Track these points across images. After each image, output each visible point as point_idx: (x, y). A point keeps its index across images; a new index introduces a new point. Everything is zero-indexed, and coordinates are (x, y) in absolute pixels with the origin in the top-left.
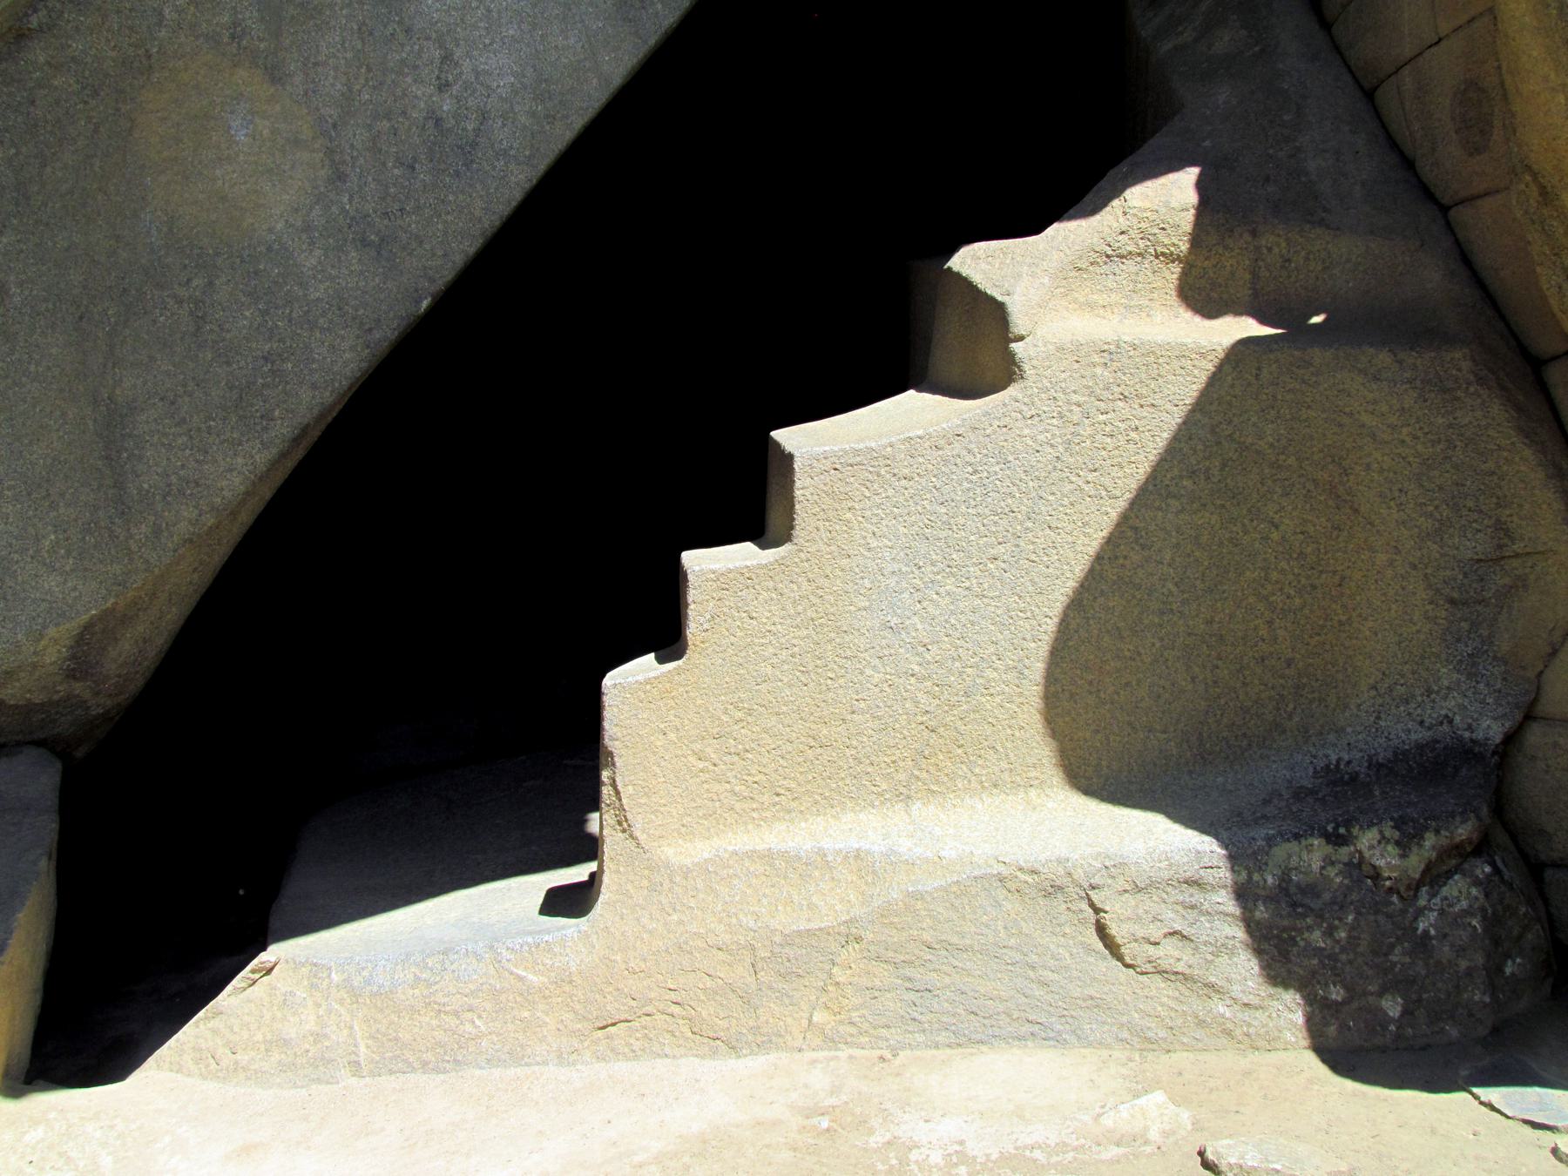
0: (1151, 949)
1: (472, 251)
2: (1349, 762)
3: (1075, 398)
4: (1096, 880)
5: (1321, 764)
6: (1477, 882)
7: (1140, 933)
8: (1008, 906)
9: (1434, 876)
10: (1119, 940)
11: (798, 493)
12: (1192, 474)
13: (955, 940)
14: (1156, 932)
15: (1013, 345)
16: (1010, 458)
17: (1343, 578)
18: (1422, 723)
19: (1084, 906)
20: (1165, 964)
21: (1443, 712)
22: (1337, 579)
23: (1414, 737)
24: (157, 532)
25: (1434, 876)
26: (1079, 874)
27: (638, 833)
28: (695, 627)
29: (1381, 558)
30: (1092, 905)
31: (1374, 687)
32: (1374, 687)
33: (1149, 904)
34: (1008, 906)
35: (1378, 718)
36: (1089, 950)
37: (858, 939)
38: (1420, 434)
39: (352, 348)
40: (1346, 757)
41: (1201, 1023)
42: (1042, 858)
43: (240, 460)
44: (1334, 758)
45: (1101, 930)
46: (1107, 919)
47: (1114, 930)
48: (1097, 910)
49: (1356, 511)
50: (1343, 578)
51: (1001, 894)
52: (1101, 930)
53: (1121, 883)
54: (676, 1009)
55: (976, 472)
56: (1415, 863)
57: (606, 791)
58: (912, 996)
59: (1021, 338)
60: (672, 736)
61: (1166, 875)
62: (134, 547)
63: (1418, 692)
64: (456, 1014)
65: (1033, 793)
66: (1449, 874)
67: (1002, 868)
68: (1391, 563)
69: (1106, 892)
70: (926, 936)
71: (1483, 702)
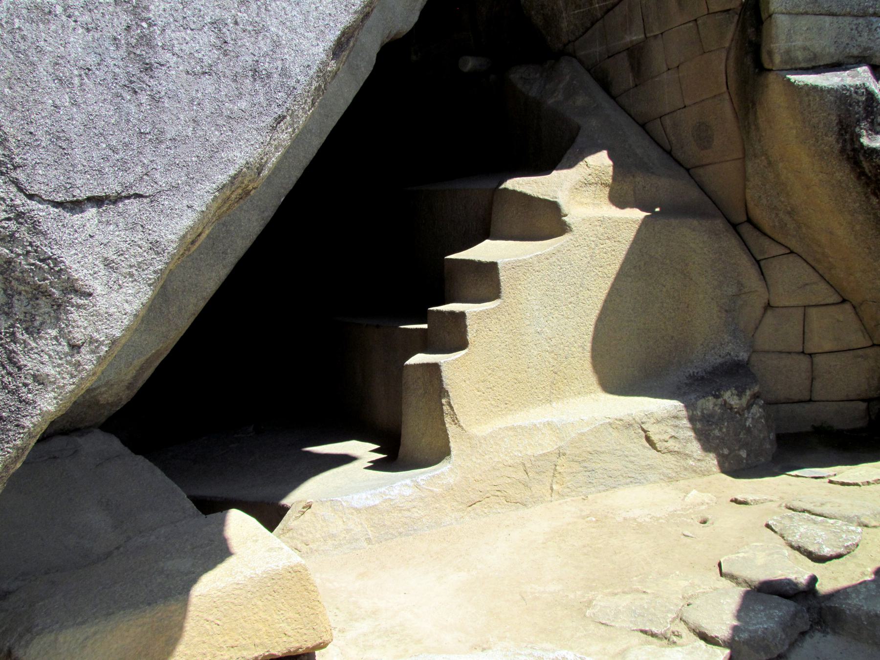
0: (666, 444)
1: (299, 175)
3: (592, 239)
4: (644, 420)
5: (687, 375)
6: (760, 407)
8: (614, 434)
11: (501, 278)
13: (599, 449)
14: (666, 437)
19: (640, 431)
20: (671, 448)
24: (180, 310)
25: (749, 406)
26: (637, 419)
27: (462, 424)
28: (471, 336)
29: (701, 296)
30: (643, 430)
33: (662, 427)
34: (614, 434)
36: (644, 447)
37: (564, 454)
39: (257, 220)
41: (686, 469)
42: (622, 414)
43: (214, 274)
44: (691, 372)
45: (648, 439)
46: (650, 434)
47: (654, 438)
48: (645, 431)
51: (611, 430)
52: (648, 439)
53: (652, 420)
54: (498, 493)
56: (744, 401)
57: (446, 408)
58: (588, 473)
60: (468, 382)
61: (666, 415)
62: (171, 318)
64: (409, 510)
65: (593, 395)
66: (752, 405)
67: (608, 420)
68: (704, 298)
70: (589, 449)
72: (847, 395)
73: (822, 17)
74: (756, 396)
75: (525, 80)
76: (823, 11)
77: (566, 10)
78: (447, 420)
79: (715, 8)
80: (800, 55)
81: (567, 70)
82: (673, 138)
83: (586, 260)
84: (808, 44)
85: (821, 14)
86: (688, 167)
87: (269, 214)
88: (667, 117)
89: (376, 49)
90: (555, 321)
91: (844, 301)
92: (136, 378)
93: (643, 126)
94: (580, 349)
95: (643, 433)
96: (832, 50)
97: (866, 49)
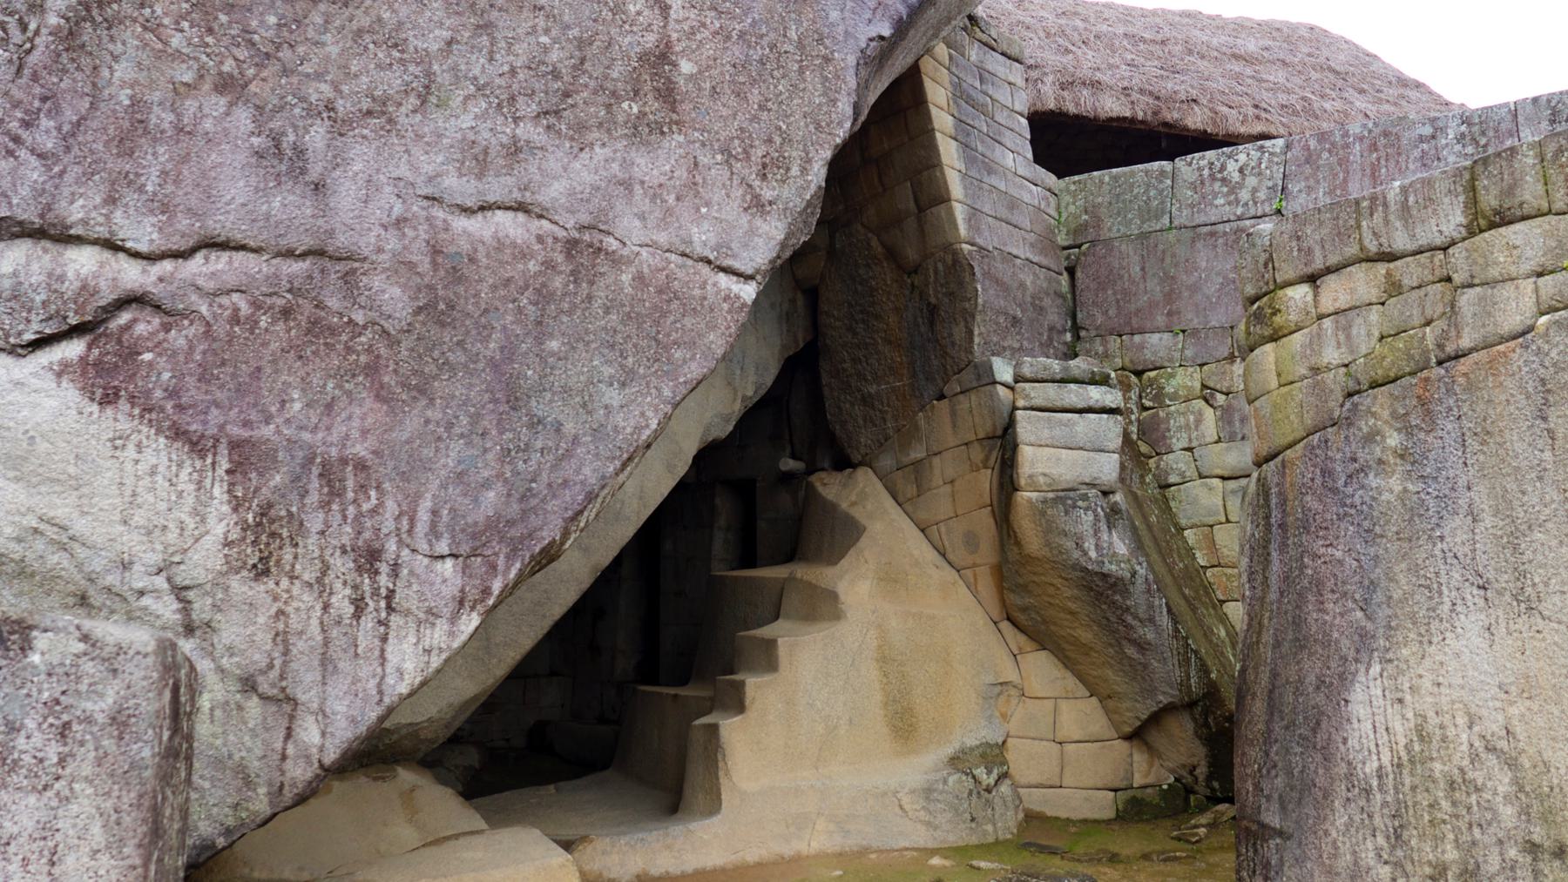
45: (901, 807)
52: (901, 807)
57: (721, 764)
75: (830, 486)
78: (721, 774)
79: (981, 435)
80: (1041, 479)
81: (865, 479)
87: (586, 585)
89: (694, 451)
92: (454, 718)
93: (923, 531)
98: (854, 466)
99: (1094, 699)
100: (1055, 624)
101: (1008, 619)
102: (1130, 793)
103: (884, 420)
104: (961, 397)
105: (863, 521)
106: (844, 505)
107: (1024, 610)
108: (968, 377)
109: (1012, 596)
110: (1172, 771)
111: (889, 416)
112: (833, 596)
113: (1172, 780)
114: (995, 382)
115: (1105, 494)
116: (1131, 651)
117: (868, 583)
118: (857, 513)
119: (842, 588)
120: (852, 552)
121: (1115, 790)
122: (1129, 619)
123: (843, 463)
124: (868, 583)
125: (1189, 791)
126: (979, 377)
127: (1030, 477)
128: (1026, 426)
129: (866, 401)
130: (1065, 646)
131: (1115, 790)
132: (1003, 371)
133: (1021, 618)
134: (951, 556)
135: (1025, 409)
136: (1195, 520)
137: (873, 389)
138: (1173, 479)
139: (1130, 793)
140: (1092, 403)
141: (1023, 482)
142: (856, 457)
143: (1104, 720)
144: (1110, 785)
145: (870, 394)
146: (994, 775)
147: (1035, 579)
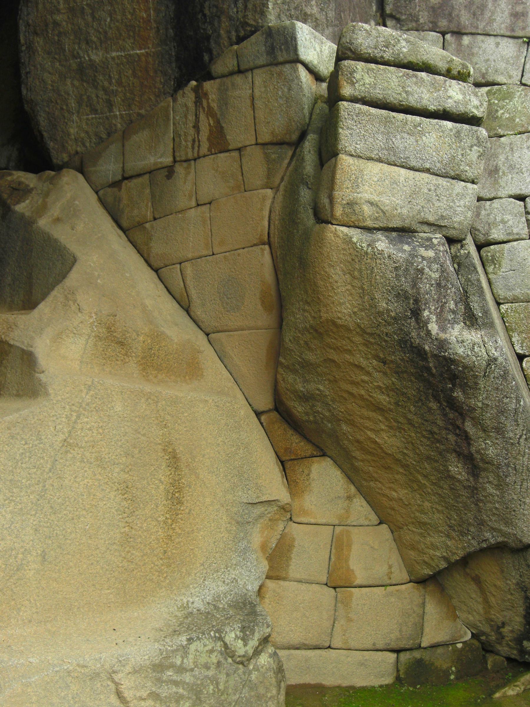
2: (193, 603)
4: (116, 668)
7: (138, 695)
9: (257, 652)
10: (128, 699)
12: (127, 455)
15: (37, 375)
16: (43, 437)
17: (190, 510)
18: (224, 582)
21: (233, 576)
22: (187, 511)
23: (221, 589)
30: (113, 681)
31: (202, 565)
32: (202, 565)
35: (205, 580)
38: (226, 441)
40: (191, 600)
44: (185, 600)
45: (119, 695)
47: (128, 694)
48: (117, 684)
49: (198, 477)
50: (190, 510)
52: (119, 695)
53: (128, 669)
55: (26, 443)
59: (43, 372)
63: (222, 567)
65: (49, 625)
69: (120, 675)
71: (250, 571)
72: (374, 644)
73: (396, 168)
74: (265, 640)
76: (398, 162)
77: (78, 112)
79: (266, 138)
80: (367, 209)
82: (193, 293)
83: (62, 437)
84: (375, 198)
85: (395, 165)
86: (207, 330)
88: (188, 264)
90: (9, 516)
91: (380, 523)
94: (40, 558)
95: (112, 686)
96: (405, 211)
97: (442, 217)
98: (58, 168)
99: (384, 526)
100: (351, 423)
101: (276, 409)
102: (417, 654)
103: (110, 105)
104: (238, 79)
105: (73, 247)
106: (43, 223)
107: (305, 398)
108: (254, 48)
109: (291, 378)
110: (469, 626)
111: (118, 100)
112: (28, 359)
113: (469, 635)
114: (297, 60)
115: (451, 241)
116: (457, 469)
117: (82, 341)
118: (62, 234)
119: (41, 348)
120: (56, 293)
121: (398, 651)
122: (469, 427)
123: (38, 159)
124: (82, 341)
125: (487, 649)
126: (271, 51)
127: (351, 204)
128: (356, 129)
129: (85, 72)
130: (357, 454)
131: (398, 651)
132: (315, 48)
133: (299, 409)
134: (198, 312)
135: (354, 100)
136: (517, 292)
137: (97, 56)
138: (496, 234)
139: (417, 654)
140: (449, 105)
141: (339, 211)
142: (59, 157)
143: (395, 559)
144: (393, 645)
145: (92, 64)
146: (253, 643)
147: (334, 355)
